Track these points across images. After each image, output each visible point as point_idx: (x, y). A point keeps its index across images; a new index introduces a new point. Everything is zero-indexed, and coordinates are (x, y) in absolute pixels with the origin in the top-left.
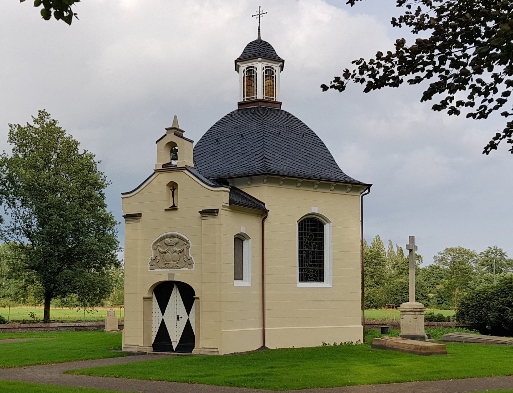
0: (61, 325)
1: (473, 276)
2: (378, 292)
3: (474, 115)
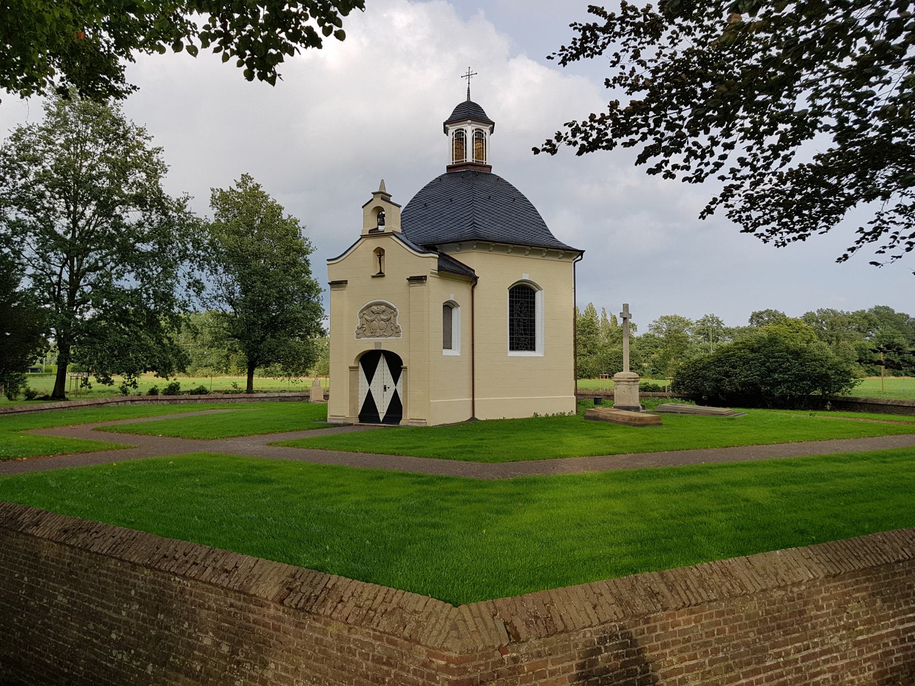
0: (265, 395)
1: (689, 345)
2: (591, 362)
3: (690, 179)
